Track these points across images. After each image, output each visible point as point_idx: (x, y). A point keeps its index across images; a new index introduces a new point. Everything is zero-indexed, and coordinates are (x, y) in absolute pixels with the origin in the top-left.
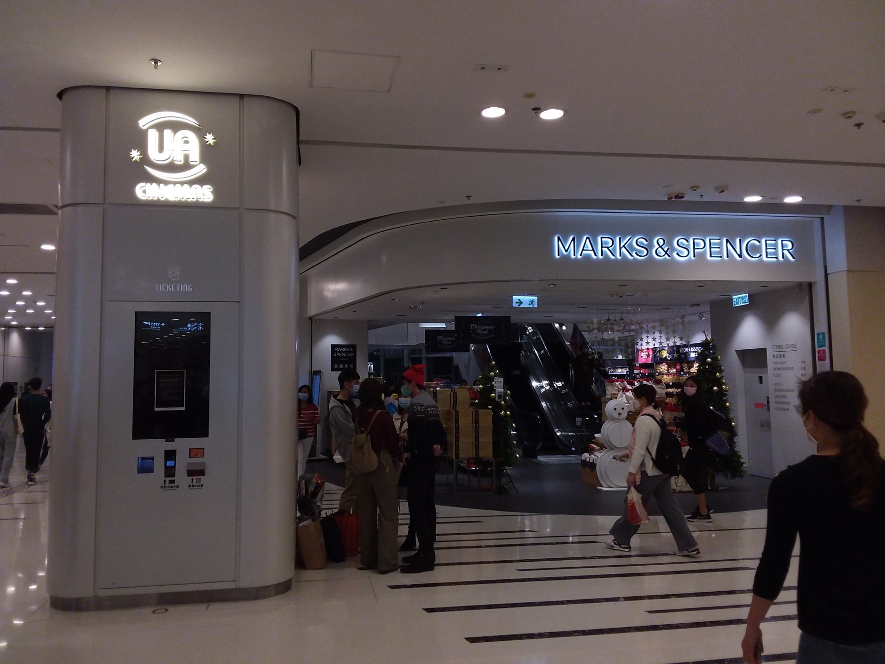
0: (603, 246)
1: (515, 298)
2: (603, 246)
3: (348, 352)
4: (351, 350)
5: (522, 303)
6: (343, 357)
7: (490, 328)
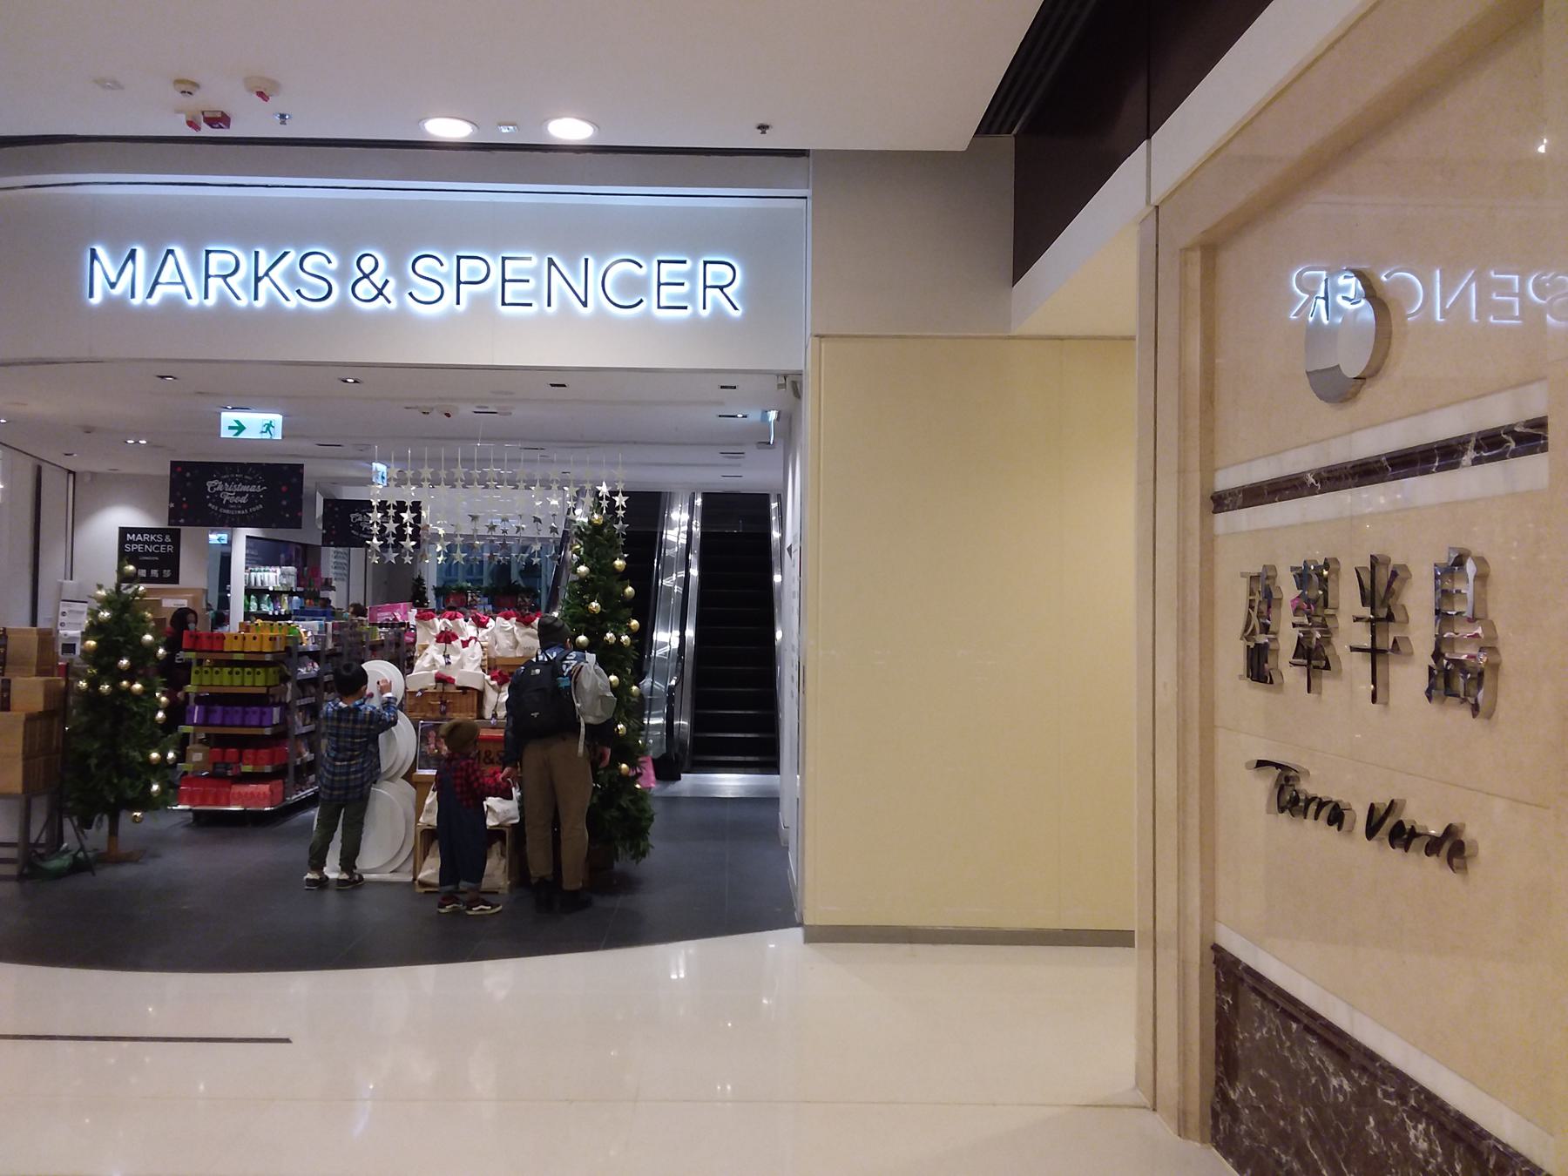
1: (228, 418)
3: (160, 544)
4: (168, 539)
5: (244, 428)
6: (147, 554)
7: (253, 489)
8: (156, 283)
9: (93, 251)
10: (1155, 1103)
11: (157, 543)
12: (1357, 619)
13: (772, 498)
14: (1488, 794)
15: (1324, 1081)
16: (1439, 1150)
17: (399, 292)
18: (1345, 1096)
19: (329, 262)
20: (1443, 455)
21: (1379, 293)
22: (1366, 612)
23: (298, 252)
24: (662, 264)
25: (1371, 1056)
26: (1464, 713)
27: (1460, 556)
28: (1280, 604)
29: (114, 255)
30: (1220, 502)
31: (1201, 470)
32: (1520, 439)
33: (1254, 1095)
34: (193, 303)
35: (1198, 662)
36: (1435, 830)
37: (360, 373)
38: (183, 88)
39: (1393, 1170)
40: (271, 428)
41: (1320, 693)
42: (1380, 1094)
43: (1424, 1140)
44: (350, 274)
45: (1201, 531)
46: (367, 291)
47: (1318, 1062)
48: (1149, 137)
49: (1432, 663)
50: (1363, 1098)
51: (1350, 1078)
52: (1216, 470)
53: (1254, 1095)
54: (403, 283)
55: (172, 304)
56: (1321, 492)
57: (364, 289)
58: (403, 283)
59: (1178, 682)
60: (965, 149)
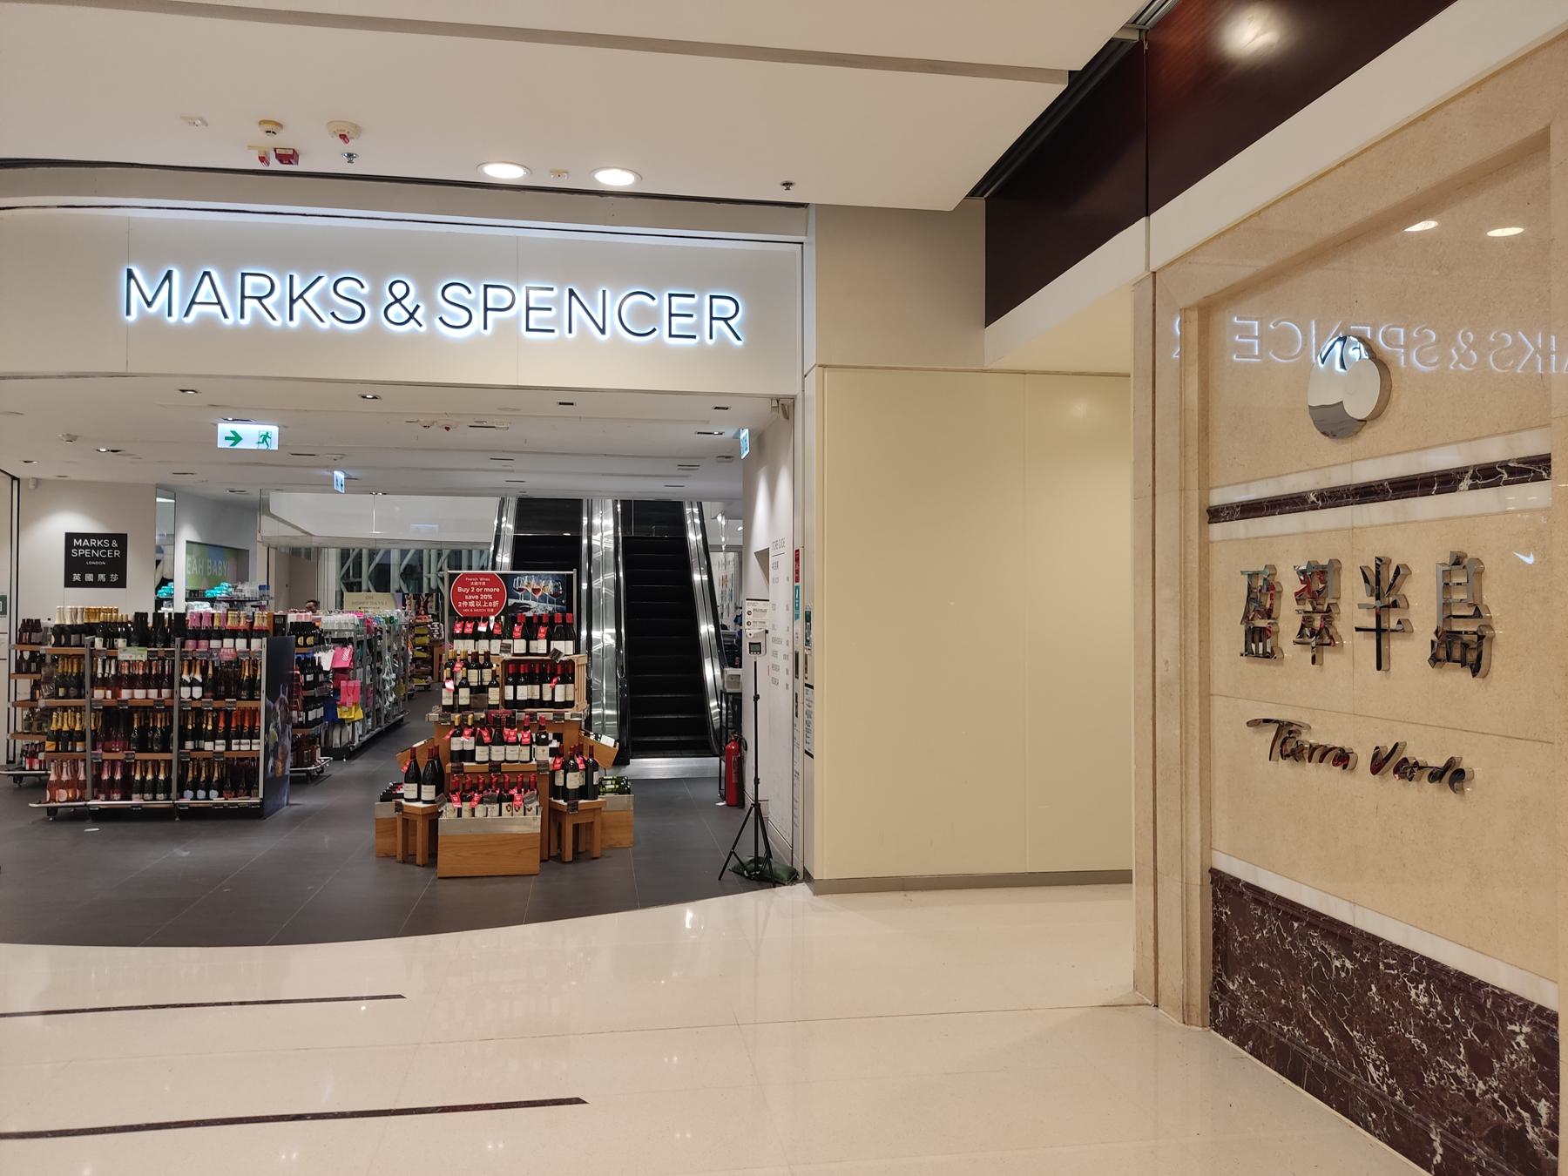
1: (224, 429)
3: (106, 549)
4: (115, 544)
5: (241, 439)
8: (193, 302)
10: (1157, 1001)
11: (105, 548)
12: (1361, 606)
13: (686, 504)
14: (1483, 733)
15: (1328, 965)
16: (1439, 1001)
17: (429, 317)
18: (1347, 973)
19: (362, 286)
20: (1446, 482)
21: (1379, 356)
22: (1372, 601)
23: (330, 277)
24: (673, 298)
25: (1375, 939)
26: (1464, 675)
27: (1458, 558)
28: (1280, 597)
29: (150, 278)
30: (1215, 514)
31: (1199, 489)
32: (1512, 471)
33: (1254, 983)
34: (228, 322)
35: (1197, 643)
36: (1438, 762)
37: (378, 390)
38: (269, 127)
39: (1395, 1023)
40: (268, 440)
41: (1322, 664)
42: (1381, 967)
43: (1425, 996)
44: (384, 298)
45: (1200, 539)
46: (398, 316)
47: (1320, 950)
48: (1148, 215)
49: (1435, 638)
50: (1366, 972)
51: (1352, 959)
52: (1212, 488)
53: (1254, 983)
54: (433, 309)
55: (206, 323)
56: (1322, 508)
57: (396, 312)
58: (433, 309)
59: (1181, 659)
60: (952, 209)
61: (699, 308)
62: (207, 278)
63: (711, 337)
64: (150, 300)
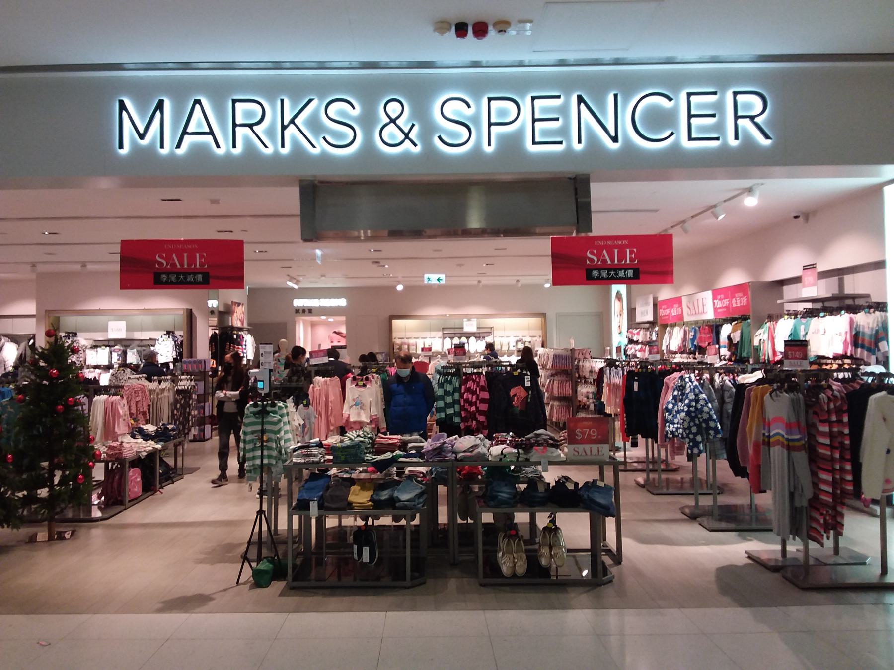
0: (740, 114)
2: (740, 114)
8: (185, 132)
9: (122, 103)
29: (141, 107)
34: (220, 152)
46: (392, 136)
61: (719, 106)
62: (198, 106)
63: (580, 142)
64: (141, 131)
